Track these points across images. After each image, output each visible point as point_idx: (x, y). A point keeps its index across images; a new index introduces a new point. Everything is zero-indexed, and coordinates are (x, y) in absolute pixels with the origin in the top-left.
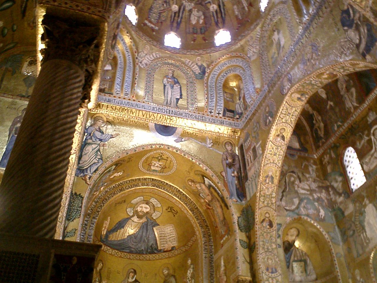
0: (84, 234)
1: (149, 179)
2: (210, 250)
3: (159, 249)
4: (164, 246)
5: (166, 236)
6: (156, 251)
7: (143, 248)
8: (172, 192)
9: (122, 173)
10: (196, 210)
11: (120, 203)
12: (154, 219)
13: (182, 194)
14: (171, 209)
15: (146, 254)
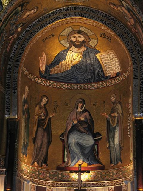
0: (9, 79)
1: (71, 8)
2: (141, 77)
3: (106, 76)
4: (109, 73)
5: (110, 63)
6: (103, 79)
7: (90, 77)
8: (98, 18)
9: (36, 10)
10: (126, 34)
11: (47, 38)
12: (94, 47)
13: (110, 18)
14: (104, 36)
15: (94, 82)
